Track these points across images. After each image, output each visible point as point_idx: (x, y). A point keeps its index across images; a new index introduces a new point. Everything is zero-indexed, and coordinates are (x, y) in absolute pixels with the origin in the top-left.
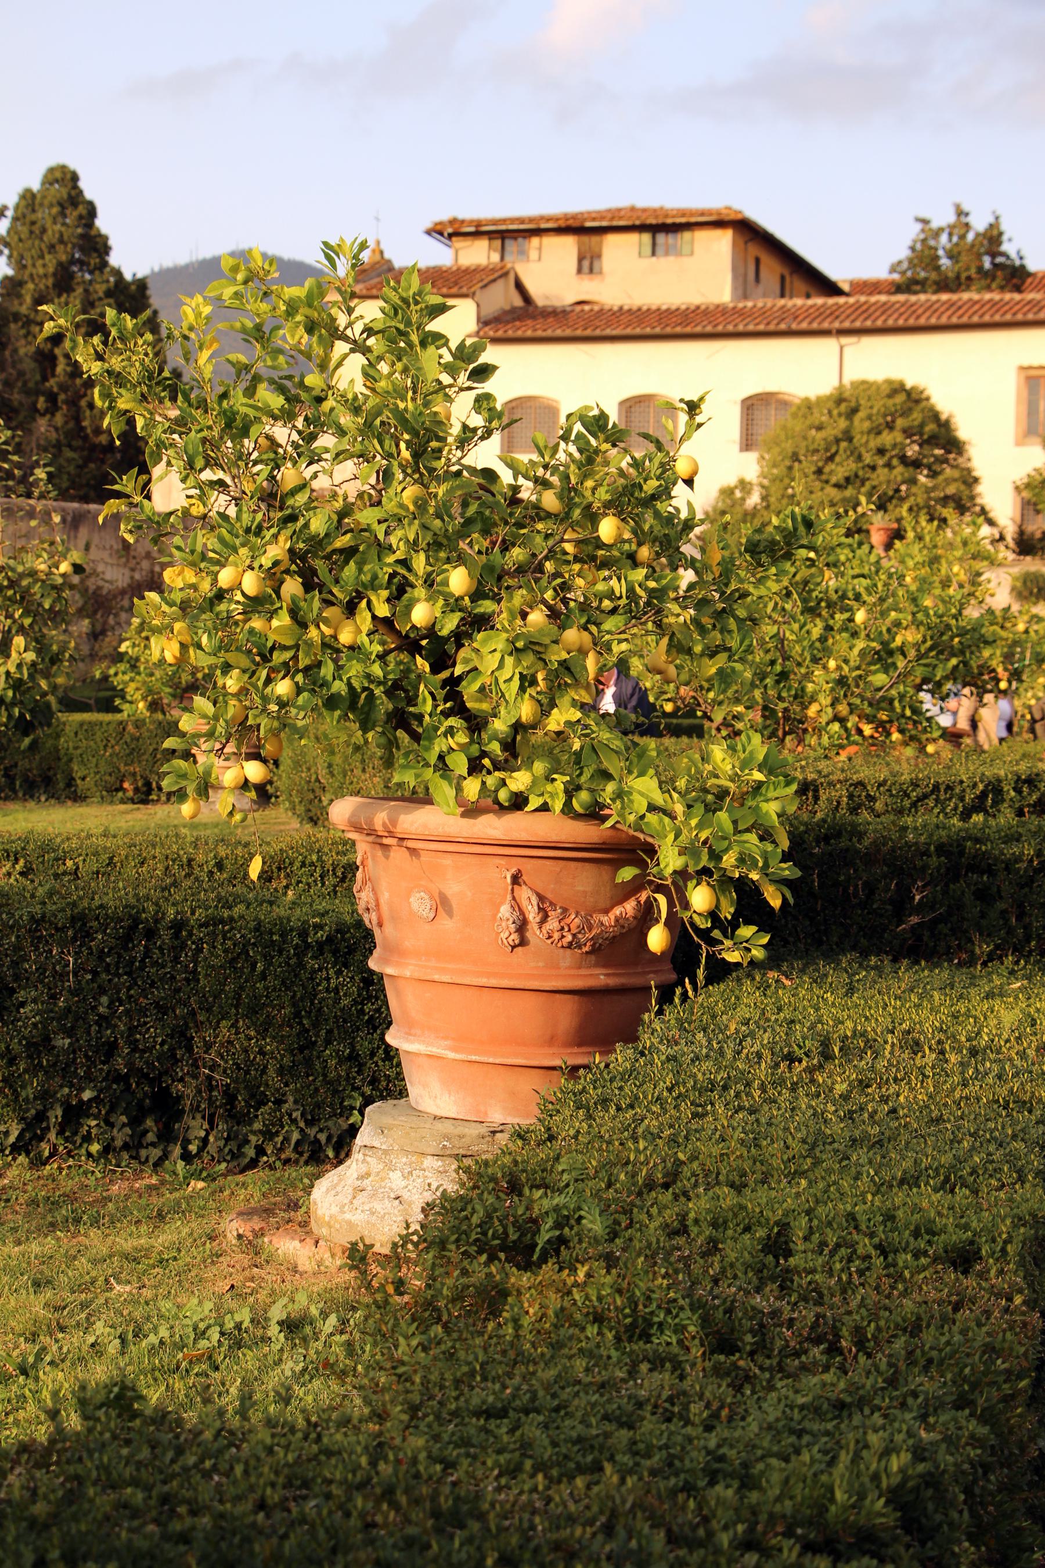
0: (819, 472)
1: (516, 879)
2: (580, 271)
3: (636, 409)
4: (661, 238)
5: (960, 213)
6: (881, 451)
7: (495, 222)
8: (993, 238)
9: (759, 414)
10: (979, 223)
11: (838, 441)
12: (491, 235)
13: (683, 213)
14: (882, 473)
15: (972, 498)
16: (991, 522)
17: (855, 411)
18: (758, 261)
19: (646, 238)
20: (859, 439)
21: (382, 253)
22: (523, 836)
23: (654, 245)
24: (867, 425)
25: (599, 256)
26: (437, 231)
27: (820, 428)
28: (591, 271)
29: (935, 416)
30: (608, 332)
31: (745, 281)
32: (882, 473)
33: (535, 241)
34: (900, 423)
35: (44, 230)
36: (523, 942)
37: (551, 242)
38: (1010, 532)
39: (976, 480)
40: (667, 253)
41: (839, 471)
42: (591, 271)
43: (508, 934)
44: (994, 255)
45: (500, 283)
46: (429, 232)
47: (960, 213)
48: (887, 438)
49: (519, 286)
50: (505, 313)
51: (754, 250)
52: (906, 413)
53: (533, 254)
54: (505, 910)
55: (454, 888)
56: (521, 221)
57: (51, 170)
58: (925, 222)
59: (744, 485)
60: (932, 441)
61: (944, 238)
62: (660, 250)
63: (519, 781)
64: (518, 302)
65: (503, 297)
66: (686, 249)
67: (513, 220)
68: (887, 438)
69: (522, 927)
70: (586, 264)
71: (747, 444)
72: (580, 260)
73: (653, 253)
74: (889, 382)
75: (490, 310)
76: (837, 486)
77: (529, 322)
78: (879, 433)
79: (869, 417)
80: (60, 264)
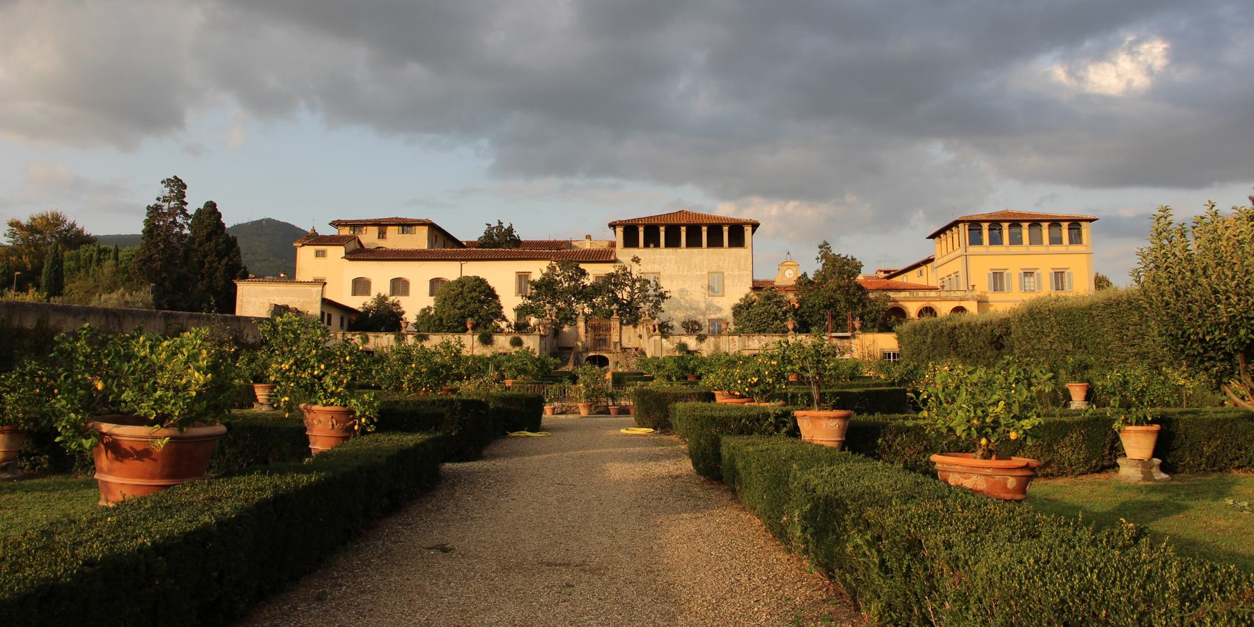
0: (453, 304)
1: (332, 417)
2: (379, 237)
3: (396, 282)
4: (405, 228)
5: (500, 223)
6: (472, 298)
8: (510, 230)
9: (436, 285)
10: (506, 226)
12: (350, 226)
13: (412, 220)
15: (501, 313)
16: (506, 321)
17: (464, 285)
18: (436, 236)
19: (400, 228)
20: (465, 294)
22: (333, 410)
23: (403, 230)
25: (386, 233)
27: (453, 290)
28: (383, 238)
29: (489, 287)
30: (387, 258)
31: (432, 243)
33: (365, 228)
35: (204, 222)
36: (333, 428)
37: (369, 228)
38: (513, 323)
39: (502, 308)
40: (407, 233)
41: (459, 304)
43: (331, 427)
45: (353, 241)
46: (330, 224)
47: (500, 223)
48: (474, 294)
49: (359, 242)
50: (354, 250)
52: (479, 287)
53: (364, 232)
54: (330, 423)
55: (321, 419)
57: (207, 202)
58: (489, 225)
59: (429, 308)
60: (487, 295)
61: (495, 230)
63: (333, 400)
64: (359, 247)
65: (353, 245)
67: (358, 221)
68: (474, 294)
69: (333, 425)
70: (381, 235)
71: (431, 294)
72: (379, 234)
73: (403, 233)
74: (474, 277)
75: (348, 250)
76: (458, 309)
77: (362, 254)
78: (471, 292)
79: (468, 288)
80: (208, 232)
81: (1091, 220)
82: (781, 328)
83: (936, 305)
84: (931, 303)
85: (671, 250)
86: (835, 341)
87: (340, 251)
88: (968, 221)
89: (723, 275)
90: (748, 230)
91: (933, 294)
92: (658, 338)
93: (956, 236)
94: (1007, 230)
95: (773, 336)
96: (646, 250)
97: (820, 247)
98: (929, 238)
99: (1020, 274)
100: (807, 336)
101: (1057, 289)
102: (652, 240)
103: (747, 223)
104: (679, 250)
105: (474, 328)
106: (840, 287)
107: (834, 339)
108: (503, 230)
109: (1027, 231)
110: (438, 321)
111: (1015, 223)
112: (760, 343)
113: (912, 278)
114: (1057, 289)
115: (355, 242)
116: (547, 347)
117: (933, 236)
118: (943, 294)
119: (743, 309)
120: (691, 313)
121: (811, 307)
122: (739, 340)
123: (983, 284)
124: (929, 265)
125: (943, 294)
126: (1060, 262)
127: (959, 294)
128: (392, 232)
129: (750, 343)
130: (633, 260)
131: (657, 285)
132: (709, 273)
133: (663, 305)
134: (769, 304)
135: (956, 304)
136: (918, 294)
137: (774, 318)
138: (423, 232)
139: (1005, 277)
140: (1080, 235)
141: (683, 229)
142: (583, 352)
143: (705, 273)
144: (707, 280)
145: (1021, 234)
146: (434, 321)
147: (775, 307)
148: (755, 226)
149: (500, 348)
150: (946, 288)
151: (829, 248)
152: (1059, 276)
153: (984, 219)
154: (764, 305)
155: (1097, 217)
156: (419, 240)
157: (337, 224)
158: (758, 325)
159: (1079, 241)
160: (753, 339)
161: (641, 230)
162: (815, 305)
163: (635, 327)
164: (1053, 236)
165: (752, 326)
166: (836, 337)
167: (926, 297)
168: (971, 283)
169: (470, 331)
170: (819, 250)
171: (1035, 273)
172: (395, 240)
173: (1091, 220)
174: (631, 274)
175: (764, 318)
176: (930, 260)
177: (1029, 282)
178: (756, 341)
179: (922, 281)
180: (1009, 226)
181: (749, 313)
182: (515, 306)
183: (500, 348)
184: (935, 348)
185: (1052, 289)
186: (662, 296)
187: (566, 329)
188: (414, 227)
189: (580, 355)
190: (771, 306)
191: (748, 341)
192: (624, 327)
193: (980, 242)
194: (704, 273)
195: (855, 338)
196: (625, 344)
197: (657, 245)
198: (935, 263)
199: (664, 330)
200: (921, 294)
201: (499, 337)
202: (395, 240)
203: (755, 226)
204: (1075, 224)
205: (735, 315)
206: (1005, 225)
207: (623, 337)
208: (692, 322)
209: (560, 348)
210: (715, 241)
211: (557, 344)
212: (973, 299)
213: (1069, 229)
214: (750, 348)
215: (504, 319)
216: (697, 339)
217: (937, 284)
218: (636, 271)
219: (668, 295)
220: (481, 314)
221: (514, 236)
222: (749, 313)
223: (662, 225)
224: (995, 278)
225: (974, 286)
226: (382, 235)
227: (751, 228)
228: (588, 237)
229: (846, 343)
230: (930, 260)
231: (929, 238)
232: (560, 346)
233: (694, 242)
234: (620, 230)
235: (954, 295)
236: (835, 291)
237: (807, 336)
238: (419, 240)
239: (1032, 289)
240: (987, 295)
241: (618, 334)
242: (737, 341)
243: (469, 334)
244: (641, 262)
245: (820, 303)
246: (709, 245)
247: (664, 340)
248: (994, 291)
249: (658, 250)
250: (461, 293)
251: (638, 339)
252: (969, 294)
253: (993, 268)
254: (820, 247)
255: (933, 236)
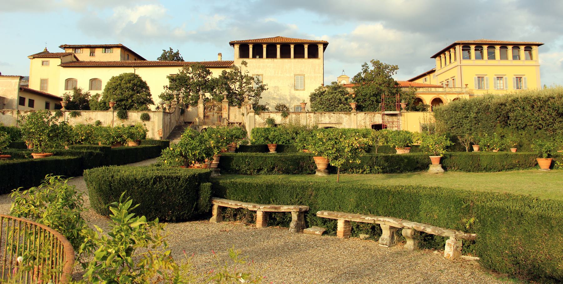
2: (90, 55)
4: (107, 50)
5: (171, 49)
7: (74, 45)
8: (177, 54)
10: (175, 51)
11: (118, 86)
14: (127, 92)
16: (154, 104)
17: (123, 79)
19: (104, 49)
21: (47, 50)
23: (105, 50)
24: (124, 82)
25: (94, 52)
26: (61, 47)
28: (93, 55)
29: (141, 81)
30: (87, 65)
32: (127, 92)
34: (132, 82)
37: (85, 50)
39: (151, 95)
42: (93, 55)
44: (177, 57)
45: (69, 57)
47: (171, 49)
48: (128, 85)
49: (75, 57)
51: (127, 53)
56: (79, 45)
61: (168, 54)
62: (106, 51)
64: (75, 60)
65: (69, 59)
66: (112, 52)
67: (77, 45)
68: (128, 85)
70: (92, 54)
72: (90, 53)
73: (105, 52)
75: (63, 62)
78: (127, 84)
79: (125, 81)
81: (538, 45)
82: (344, 109)
83: (442, 97)
84: (440, 95)
85: (270, 60)
86: (386, 118)
87: (58, 61)
88: (462, 44)
89: (304, 76)
90: (321, 47)
91: (441, 90)
92: (252, 114)
93: (443, 60)
94: (487, 50)
95: (340, 113)
96: (254, 60)
97: (363, 66)
98: (433, 57)
99: (494, 78)
100: (365, 114)
101: (518, 88)
102: (258, 53)
103: (320, 43)
104: (275, 60)
105: (115, 109)
106: (384, 82)
107: (386, 116)
108: (173, 54)
109: (499, 51)
110: (103, 104)
111: (491, 46)
112: (330, 118)
113: (420, 81)
114: (518, 88)
115: (71, 57)
116: (172, 121)
117: (435, 57)
118: (448, 90)
119: (317, 96)
120: (282, 102)
121: (364, 96)
122: (314, 116)
123: (473, 86)
124: (432, 75)
125: (448, 90)
126: (519, 71)
127: (457, 90)
128: (98, 51)
129: (323, 119)
130: (242, 64)
131: (258, 80)
132: (295, 75)
133: (263, 94)
134: (336, 93)
135: (455, 96)
136: (431, 89)
137: (339, 102)
138: (118, 51)
139: (485, 80)
140: (531, 54)
141: (278, 47)
142: (199, 125)
143: (292, 75)
144: (293, 79)
145: (494, 53)
146: (100, 104)
147: (340, 95)
148: (325, 45)
149: (133, 122)
150: (450, 86)
151: (367, 67)
152: (519, 79)
153: (474, 42)
154: (332, 93)
155: (543, 43)
156: (116, 56)
157: (65, 47)
158: (328, 107)
159: (529, 58)
160: (325, 116)
161: (251, 47)
162: (367, 94)
163: (239, 108)
164: (514, 55)
165: (323, 108)
166: (387, 115)
167: (437, 92)
168: (464, 83)
169: (112, 109)
170: (362, 68)
171: (504, 78)
172: (100, 56)
173: (538, 45)
174: (241, 73)
175: (332, 102)
176: (433, 71)
177: (500, 83)
178: (327, 117)
179: (428, 83)
180: (488, 47)
181: (321, 99)
182: (160, 94)
183: (133, 122)
184: (478, 122)
185: (514, 87)
186: (262, 88)
187: (190, 109)
188: (112, 49)
189: (197, 128)
190: (337, 94)
191: (321, 117)
192: (231, 108)
193: (470, 58)
194: (291, 75)
195: (401, 116)
196: (231, 120)
197: (261, 57)
198: (436, 73)
199: (259, 109)
200: (433, 89)
201: (133, 113)
202: (100, 56)
203: (325, 45)
204: (529, 47)
205: (311, 101)
206: (485, 47)
207: (231, 115)
208: (282, 106)
209: (185, 123)
210: (299, 54)
211: (184, 120)
212: (467, 93)
213: (525, 50)
214: (322, 122)
215: (152, 103)
216: (282, 115)
217: (439, 84)
218: (244, 71)
219: (266, 87)
220: (133, 99)
221: (180, 57)
222: (321, 99)
223: (265, 43)
224: (479, 81)
225: (467, 85)
226: (92, 54)
227: (322, 46)
228: (220, 54)
229: (395, 119)
230: (433, 71)
231: (433, 57)
232: (185, 121)
233: (285, 54)
234: (237, 47)
235: (454, 90)
236: (380, 85)
237: (365, 114)
238: (116, 56)
239: (502, 88)
240: (473, 91)
241: (227, 113)
242: (312, 117)
243: (110, 111)
244: (248, 65)
245: (371, 93)
246: (295, 57)
247: (257, 116)
248: (479, 88)
249: (261, 60)
250: (120, 84)
251: (241, 116)
252: (464, 90)
253: (478, 74)
254: (363, 66)
255: (435, 57)
